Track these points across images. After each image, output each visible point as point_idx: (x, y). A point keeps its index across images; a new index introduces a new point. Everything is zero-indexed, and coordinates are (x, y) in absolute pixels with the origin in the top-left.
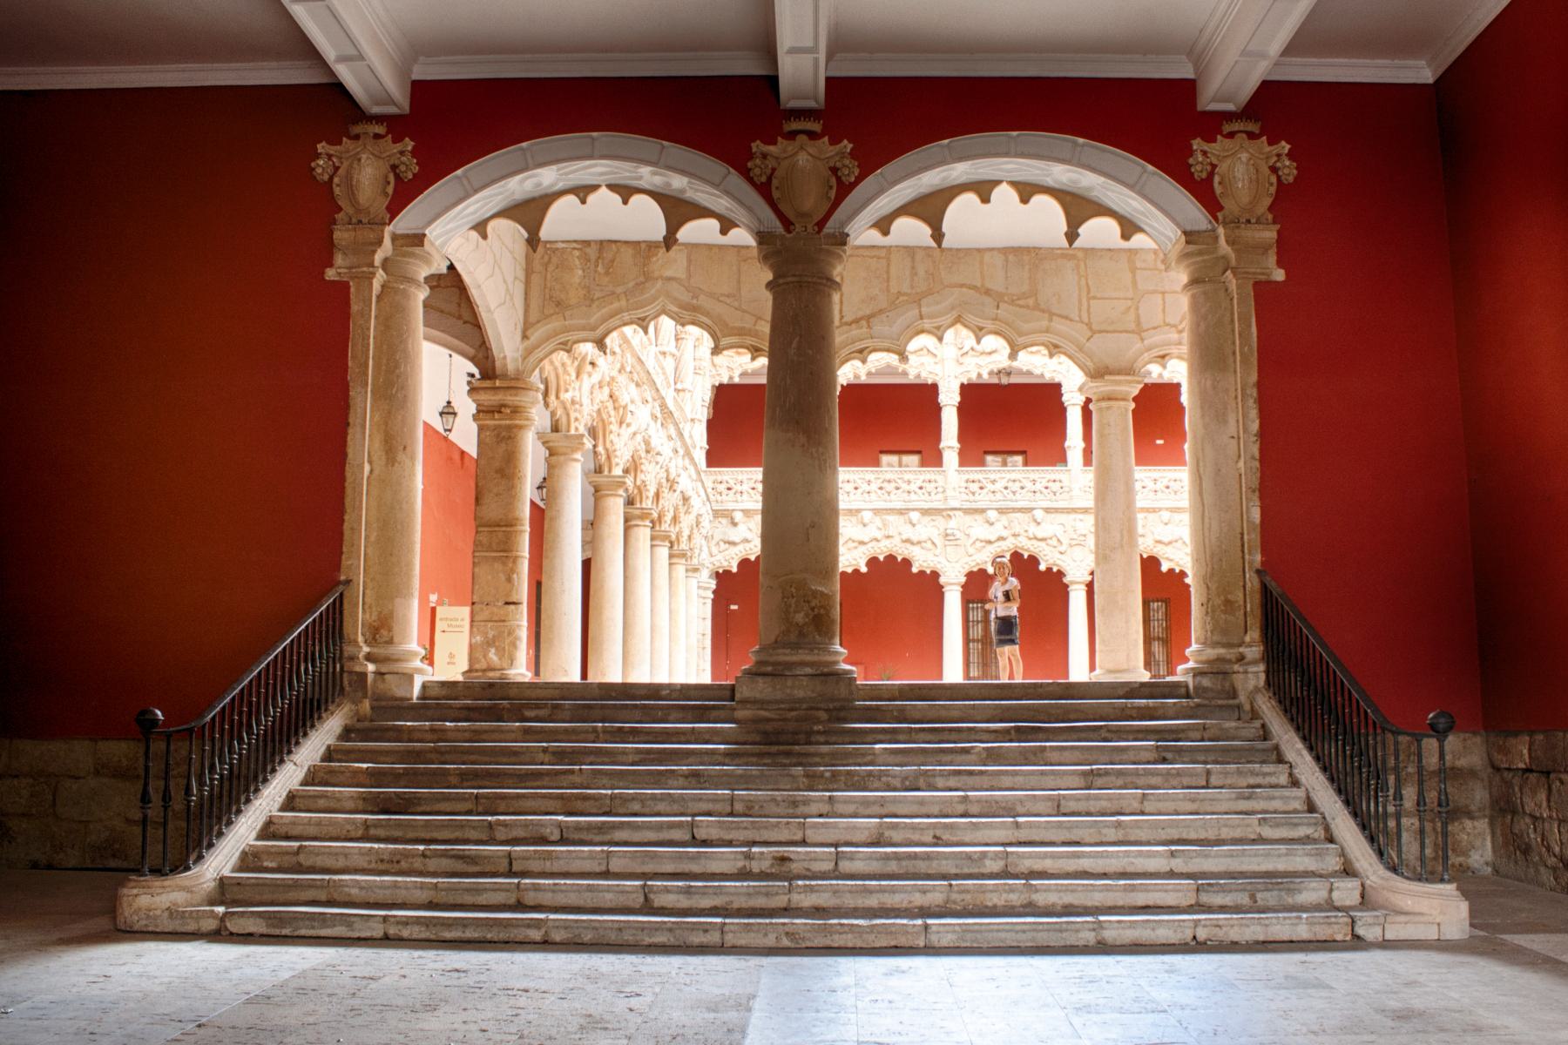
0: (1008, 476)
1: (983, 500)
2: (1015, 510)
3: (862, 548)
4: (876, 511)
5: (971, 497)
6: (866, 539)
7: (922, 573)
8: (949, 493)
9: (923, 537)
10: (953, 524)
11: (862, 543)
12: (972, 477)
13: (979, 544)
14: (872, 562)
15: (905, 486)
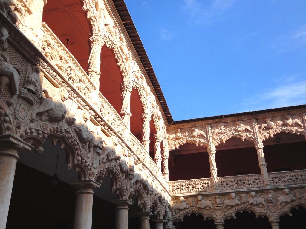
0: (290, 174)
1: (281, 185)
2: (296, 188)
3: (234, 209)
4: (237, 193)
5: (276, 184)
6: (234, 205)
7: (260, 217)
8: (266, 183)
9: (259, 202)
10: (270, 196)
11: (232, 206)
12: (274, 176)
13: (283, 204)
14: (238, 214)
15: (247, 182)
